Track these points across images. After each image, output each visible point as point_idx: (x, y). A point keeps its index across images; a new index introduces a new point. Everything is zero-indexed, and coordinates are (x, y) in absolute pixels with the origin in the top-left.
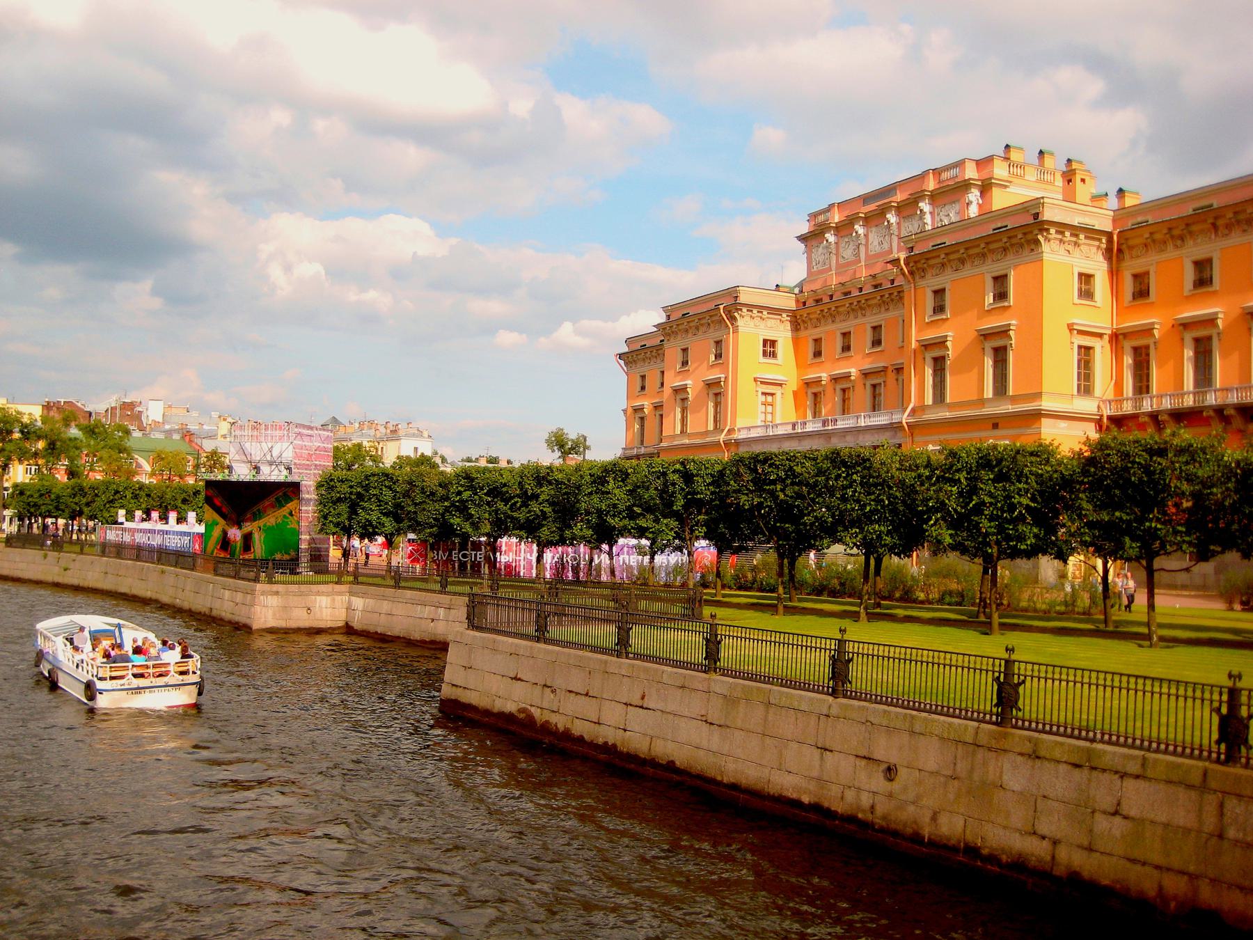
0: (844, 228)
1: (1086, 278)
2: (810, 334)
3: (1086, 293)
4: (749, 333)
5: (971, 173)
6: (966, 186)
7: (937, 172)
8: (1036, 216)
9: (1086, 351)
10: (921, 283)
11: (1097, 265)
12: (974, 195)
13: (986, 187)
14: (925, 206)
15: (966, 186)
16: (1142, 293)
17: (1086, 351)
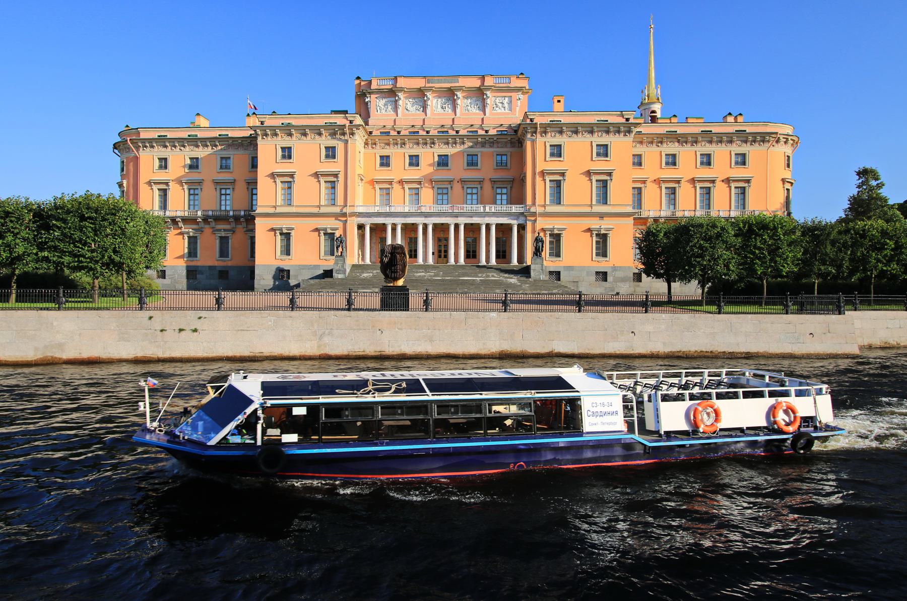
10: (544, 139)
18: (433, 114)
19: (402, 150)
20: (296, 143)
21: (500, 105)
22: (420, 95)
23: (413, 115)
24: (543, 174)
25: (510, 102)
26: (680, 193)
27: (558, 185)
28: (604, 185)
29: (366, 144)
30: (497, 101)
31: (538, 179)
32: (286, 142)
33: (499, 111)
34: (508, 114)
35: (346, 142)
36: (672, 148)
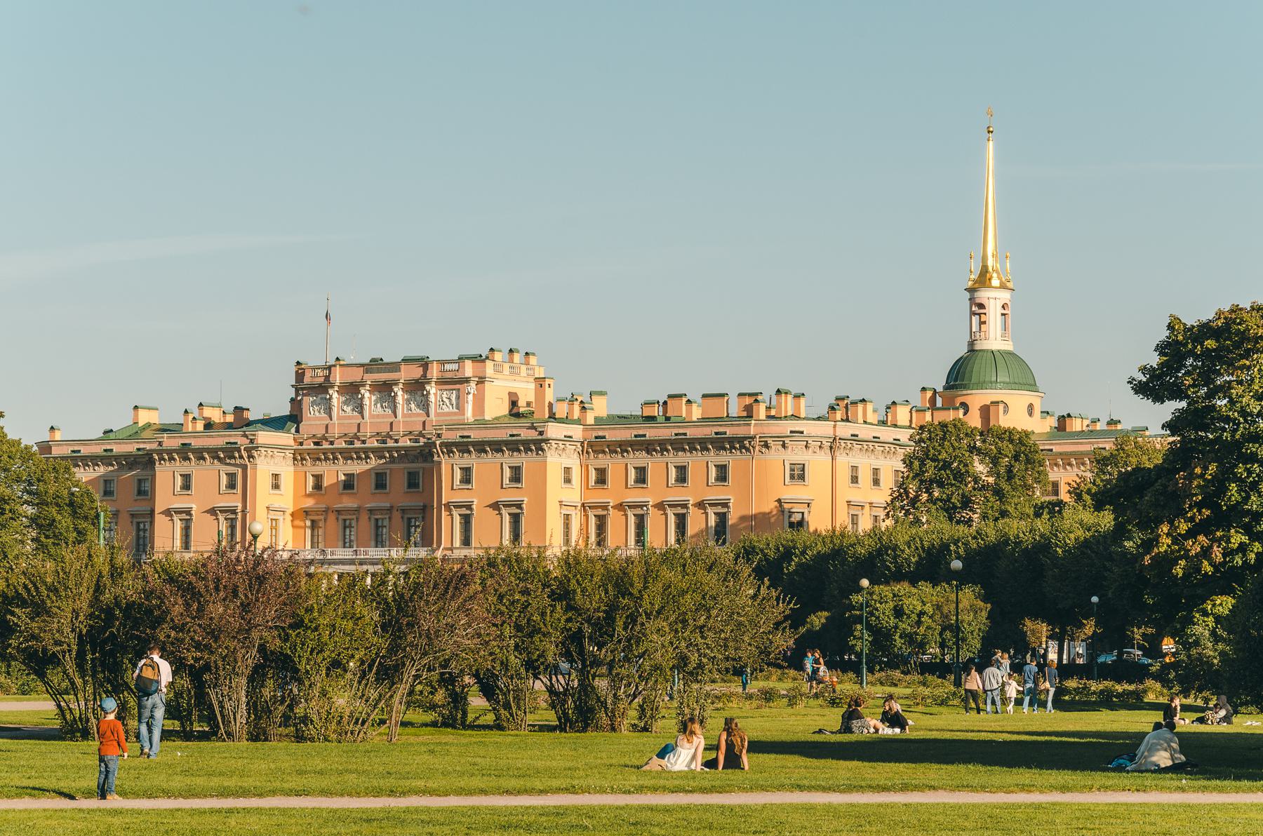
0: (351, 390)
1: (567, 470)
2: (312, 469)
3: (568, 480)
4: (264, 467)
5: (469, 369)
6: (466, 380)
7: (443, 362)
8: (541, 433)
9: (567, 517)
11: (574, 462)
12: (472, 387)
13: (481, 381)
14: (432, 389)
15: (466, 380)
16: (602, 479)
17: (567, 517)
18: (372, 416)
19: (335, 468)
20: (192, 467)
21: (447, 401)
22: (351, 390)
23: (349, 418)
24: (448, 506)
25: (458, 398)
26: (649, 523)
27: (466, 520)
28: (516, 519)
29: (295, 459)
30: (445, 396)
31: (444, 513)
32: (185, 468)
33: (446, 410)
34: (455, 414)
35: (244, 468)
36: (641, 458)
